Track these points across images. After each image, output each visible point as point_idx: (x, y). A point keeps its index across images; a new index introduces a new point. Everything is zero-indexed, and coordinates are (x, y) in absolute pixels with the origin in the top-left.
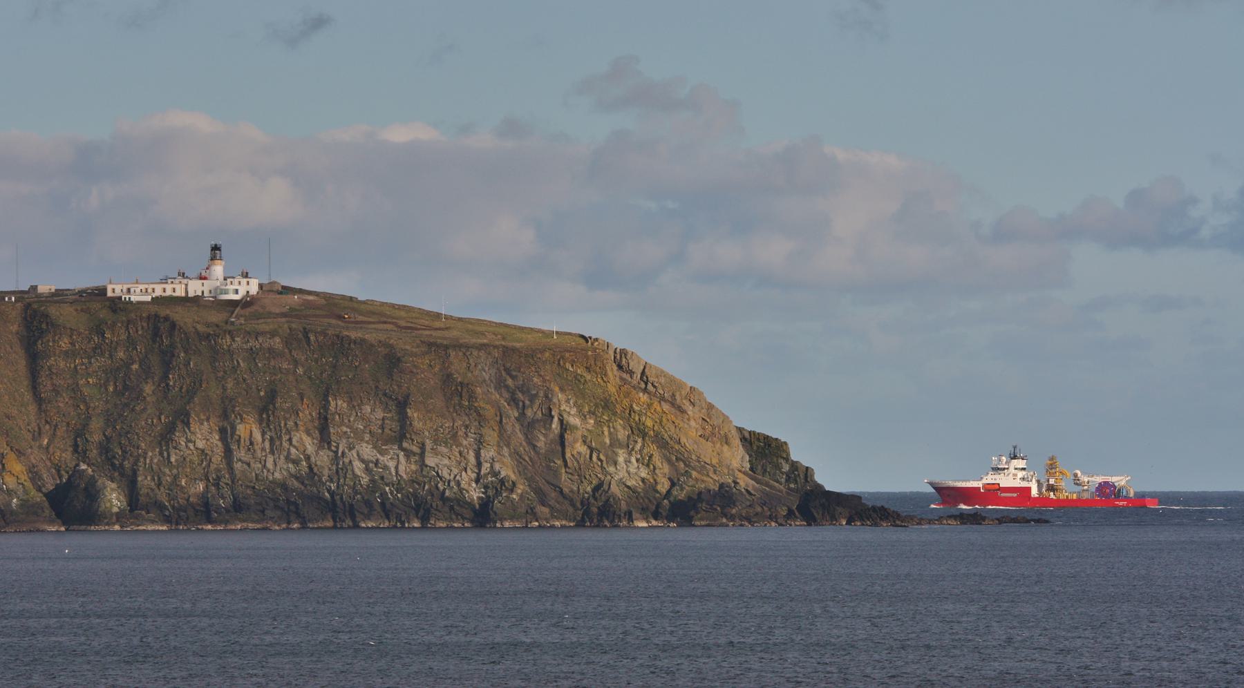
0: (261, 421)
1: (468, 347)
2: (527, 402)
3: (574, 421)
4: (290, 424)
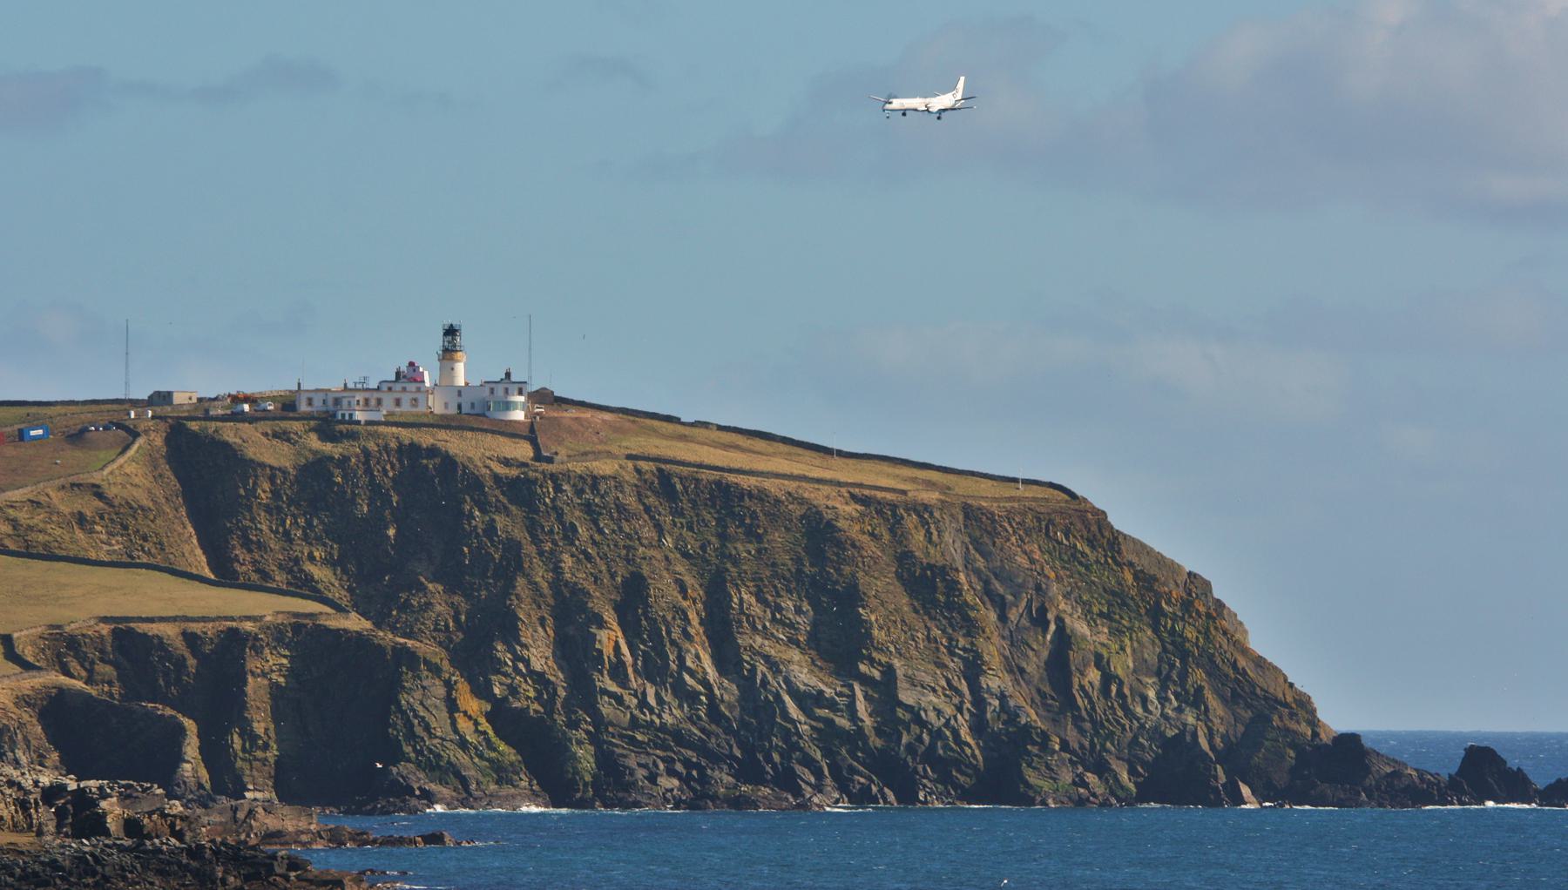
0: (623, 624)
1: (926, 507)
2: (1010, 597)
3: (1081, 628)
4: (676, 634)
